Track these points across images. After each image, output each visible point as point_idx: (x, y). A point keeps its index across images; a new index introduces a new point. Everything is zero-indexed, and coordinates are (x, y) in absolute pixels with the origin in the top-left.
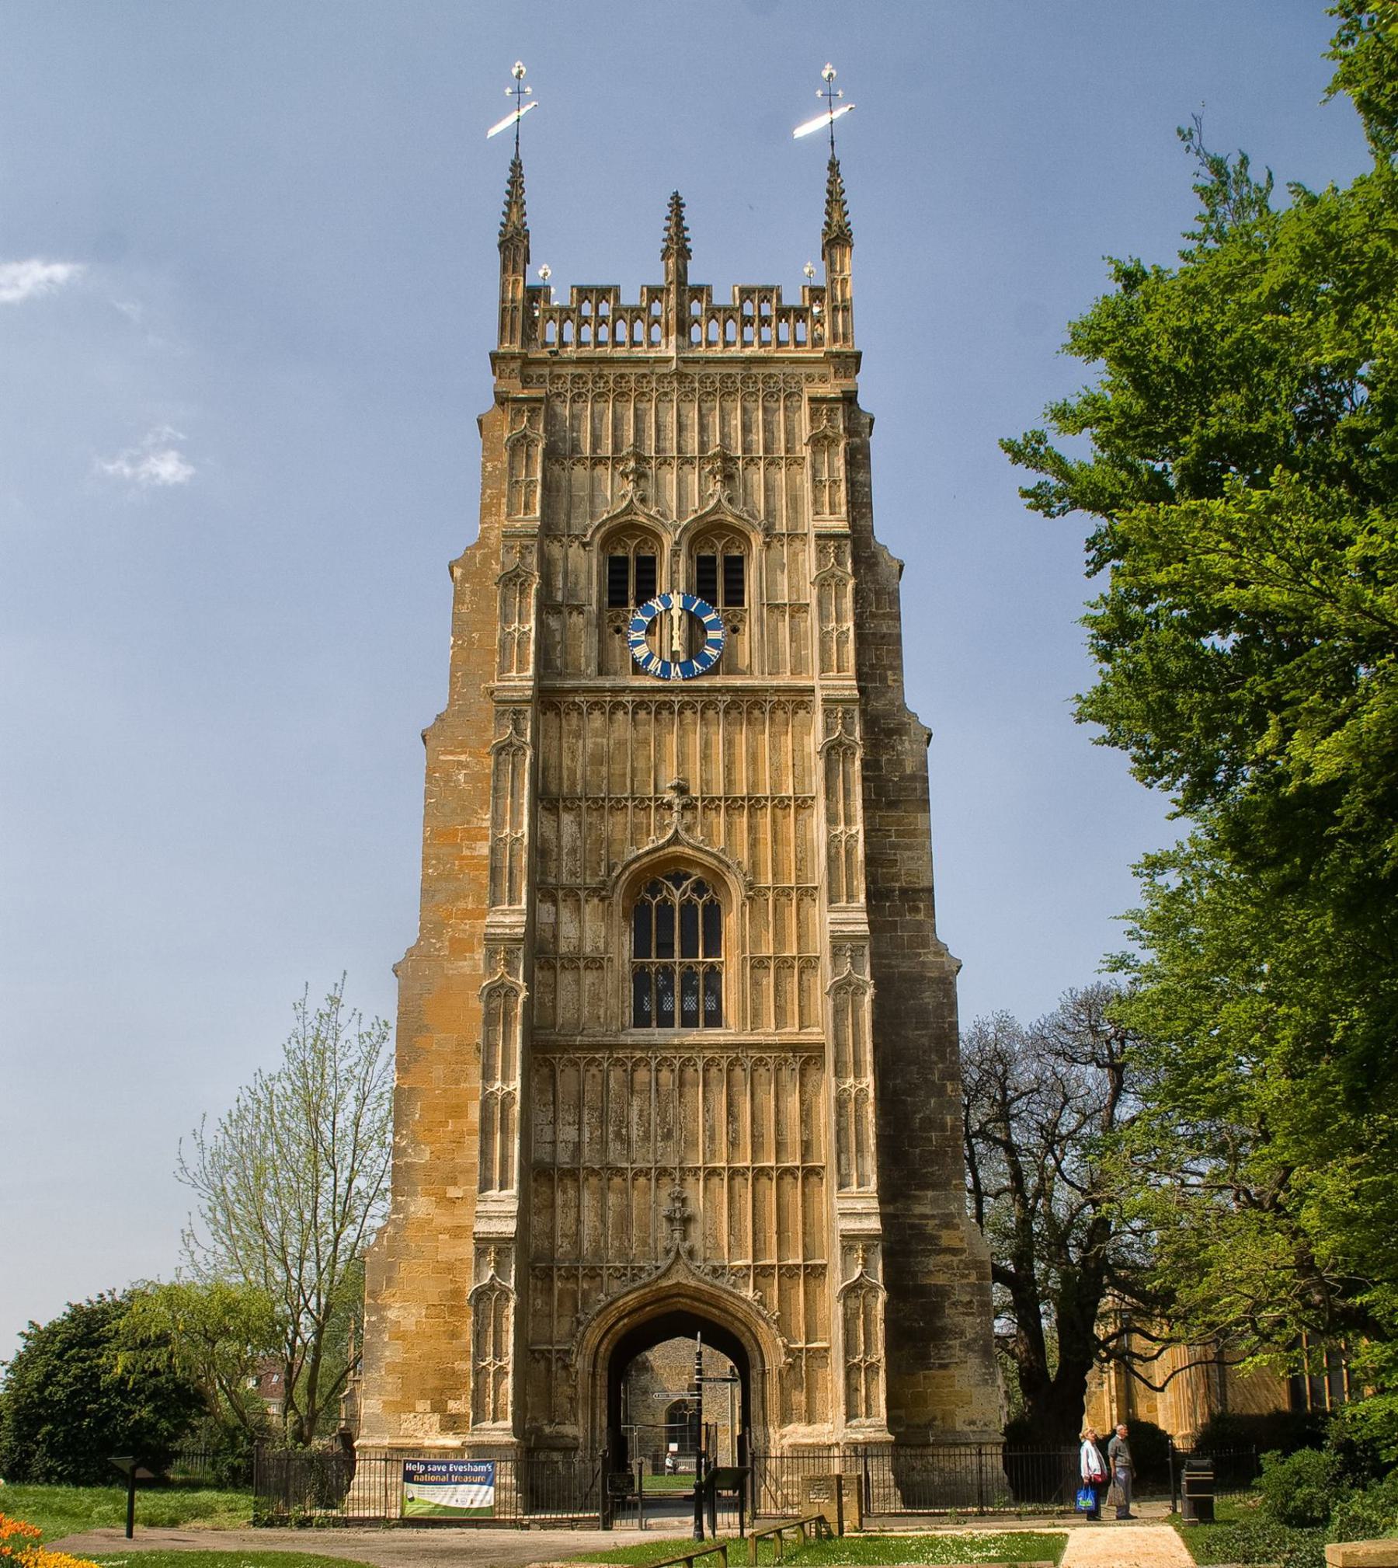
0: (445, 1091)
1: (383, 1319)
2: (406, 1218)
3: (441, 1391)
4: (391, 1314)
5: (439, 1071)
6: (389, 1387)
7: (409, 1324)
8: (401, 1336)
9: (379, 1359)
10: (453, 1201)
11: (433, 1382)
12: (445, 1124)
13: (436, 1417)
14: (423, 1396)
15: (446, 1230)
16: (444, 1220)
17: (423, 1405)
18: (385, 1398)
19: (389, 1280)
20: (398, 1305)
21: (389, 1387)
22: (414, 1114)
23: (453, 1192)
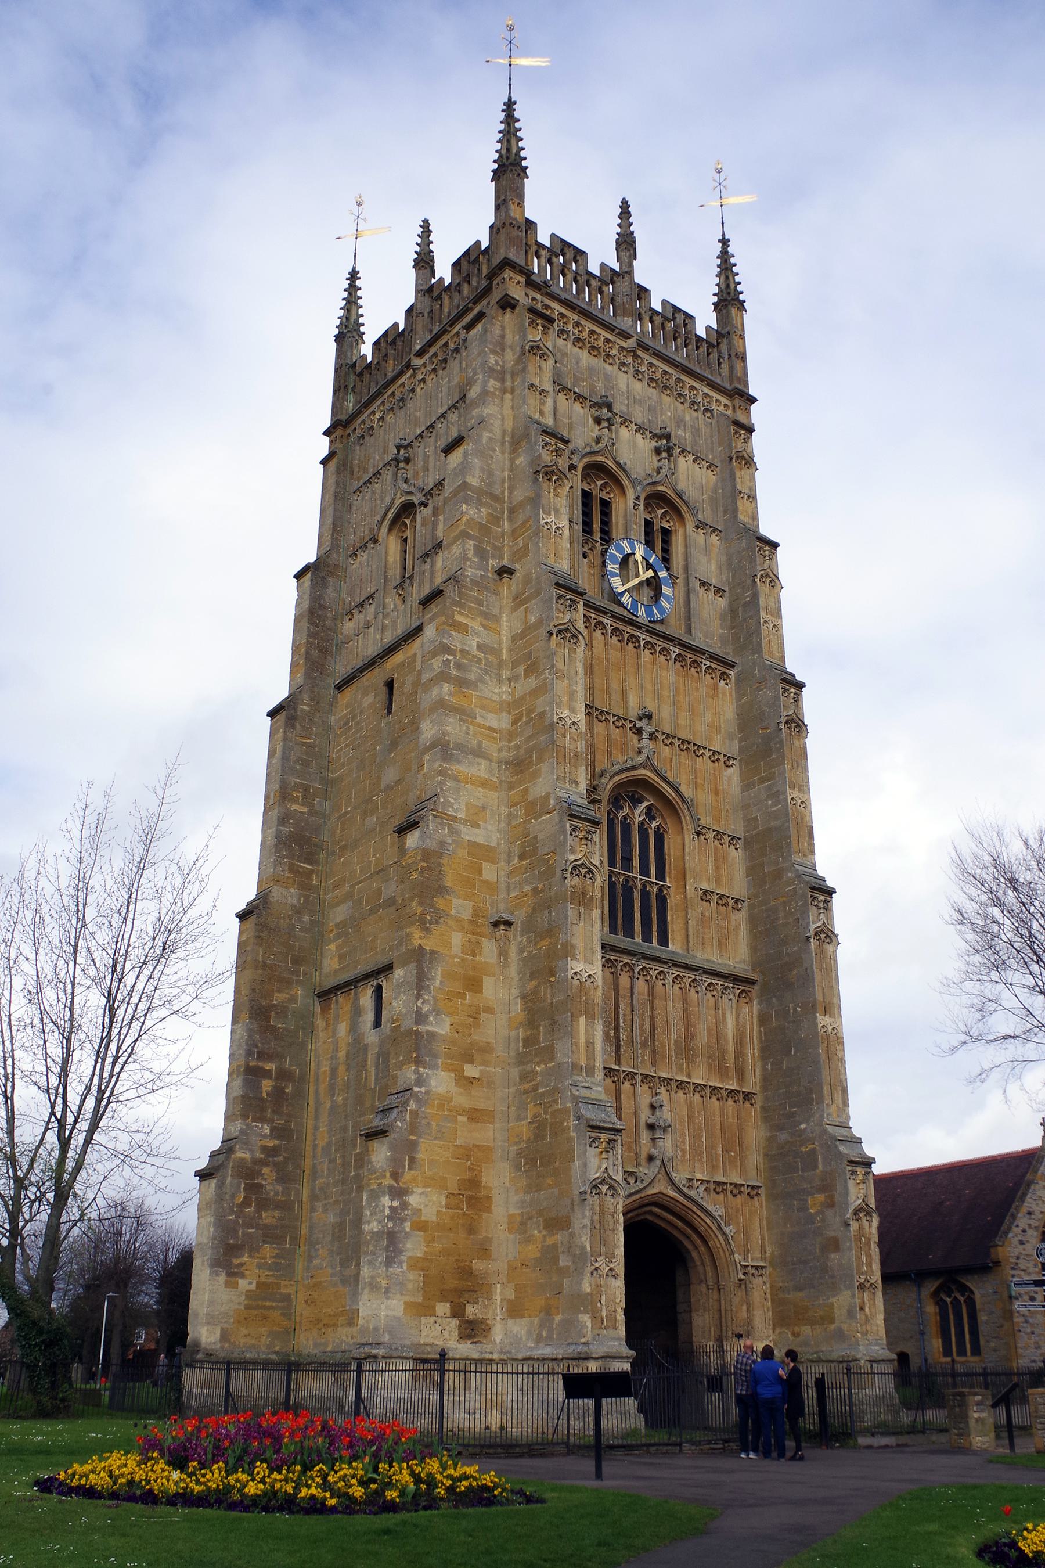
0: (463, 960)
1: (405, 1205)
2: (428, 1092)
3: (459, 1292)
4: (413, 1200)
5: (457, 939)
6: (410, 1286)
7: (430, 1214)
8: (421, 1226)
9: (401, 1252)
10: (471, 1081)
11: (453, 1283)
12: (462, 996)
13: (455, 1322)
14: (443, 1298)
15: (463, 1112)
16: (461, 1100)
17: (443, 1308)
18: (407, 1299)
19: (412, 1160)
20: (420, 1190)
21: (410, 1286)
22: (433, 979)
23: (470, 1071)
